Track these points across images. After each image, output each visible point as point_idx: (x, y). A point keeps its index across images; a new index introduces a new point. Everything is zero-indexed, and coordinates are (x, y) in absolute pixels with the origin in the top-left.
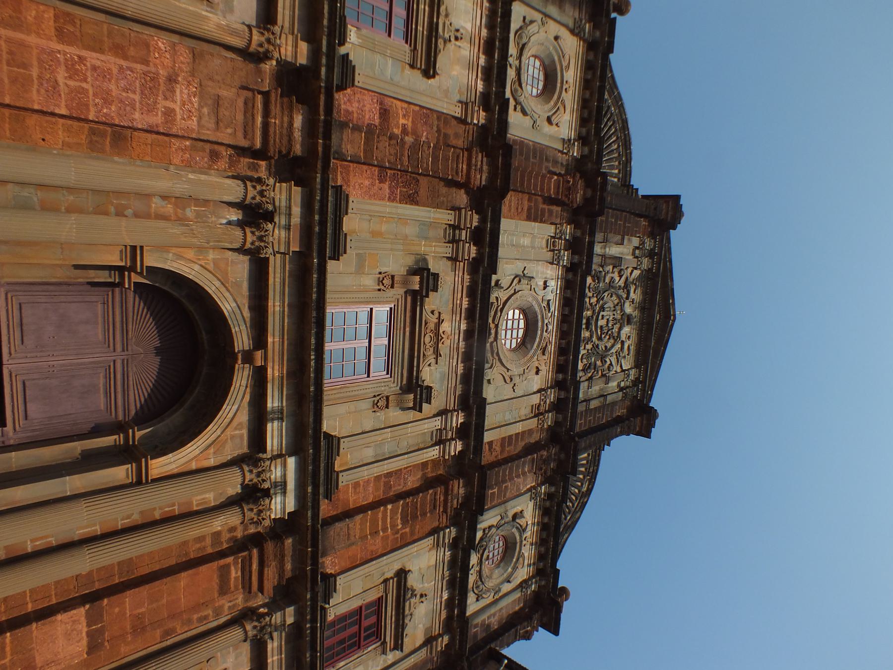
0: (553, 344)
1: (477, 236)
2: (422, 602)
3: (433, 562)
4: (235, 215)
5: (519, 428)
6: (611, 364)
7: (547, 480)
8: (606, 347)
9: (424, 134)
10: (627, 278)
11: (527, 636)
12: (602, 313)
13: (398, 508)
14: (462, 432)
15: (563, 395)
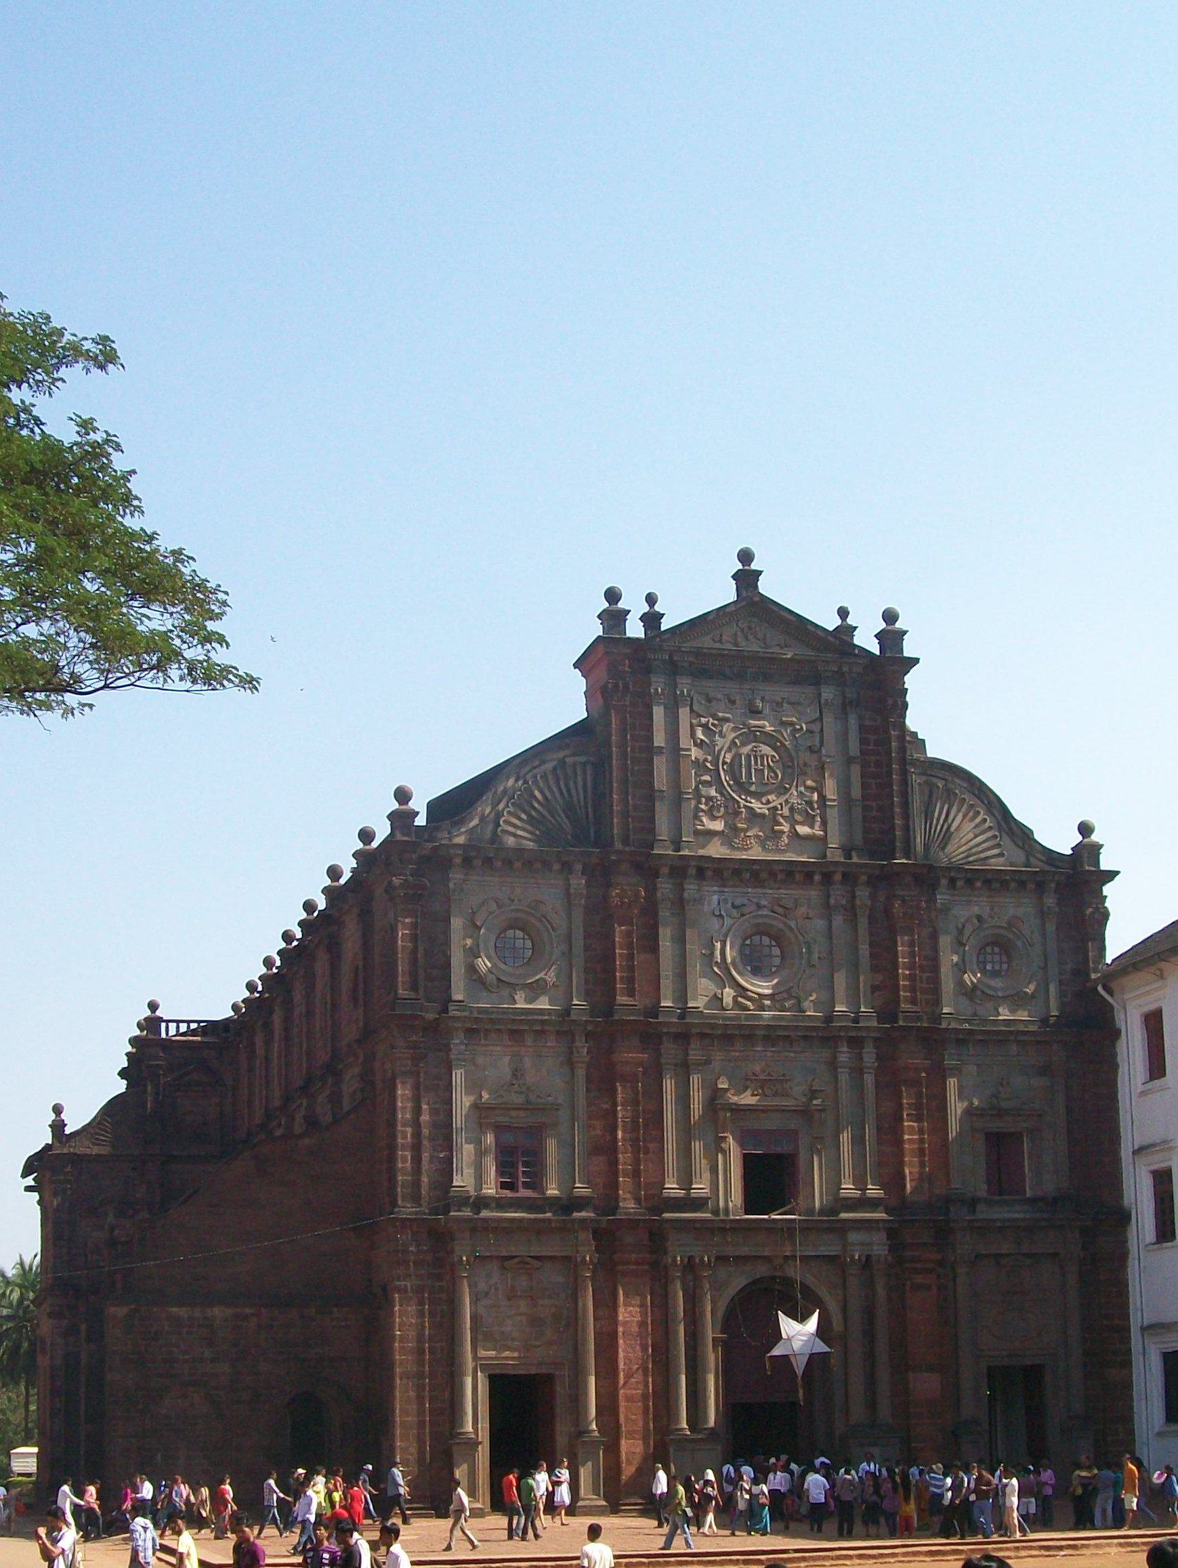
0: (782, 891)
1: (683, 1037)
2: (1008, 1083)
3: (972, 1069)
4: (690, 1277)
5: (864, 949)
6: (810, 747)
7: (934, 886)
8: (789, 767)
9: (605, 1106)
10: (705, 727)
11: (1105, 915)
12: (746, 786)
13: (909, 1126)
14: (856, 1042)
15: (838, 877)
